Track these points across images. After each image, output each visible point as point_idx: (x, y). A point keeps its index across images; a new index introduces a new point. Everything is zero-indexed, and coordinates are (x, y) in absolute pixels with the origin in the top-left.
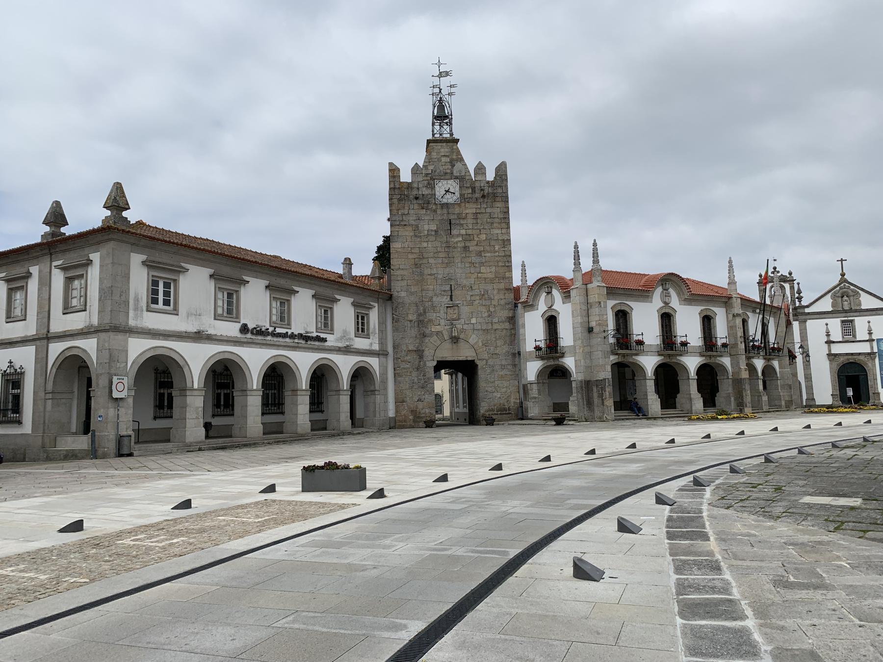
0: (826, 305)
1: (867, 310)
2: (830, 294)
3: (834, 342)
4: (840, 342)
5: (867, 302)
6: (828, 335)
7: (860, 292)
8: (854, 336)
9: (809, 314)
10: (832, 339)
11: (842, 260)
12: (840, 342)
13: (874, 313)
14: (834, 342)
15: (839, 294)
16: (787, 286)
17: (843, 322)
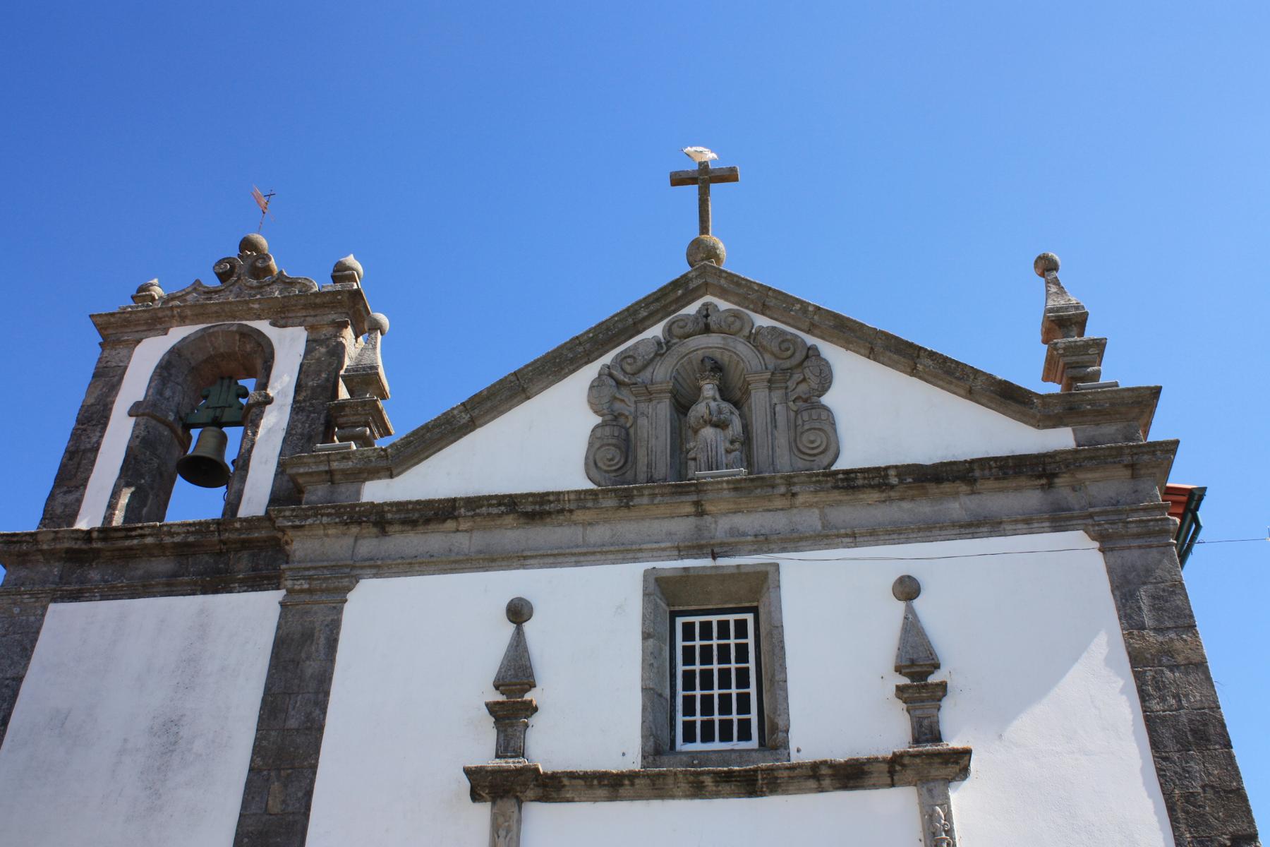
0: (547, 442)
1: (875, 480)
2: (590, 372)
3: (553, 787)
4: (610, 785)
5: (877, 416)
6: (512, 705)
7: (831, 352)
8: (773, 735)
9: (383, 519)
10: (548, 748)
11: (704, 178)
12: (610, 785)
13: (958, 506)
14: (553, 787)
15: (662, 373)
16: (289, 347)
17: (668, 597)
